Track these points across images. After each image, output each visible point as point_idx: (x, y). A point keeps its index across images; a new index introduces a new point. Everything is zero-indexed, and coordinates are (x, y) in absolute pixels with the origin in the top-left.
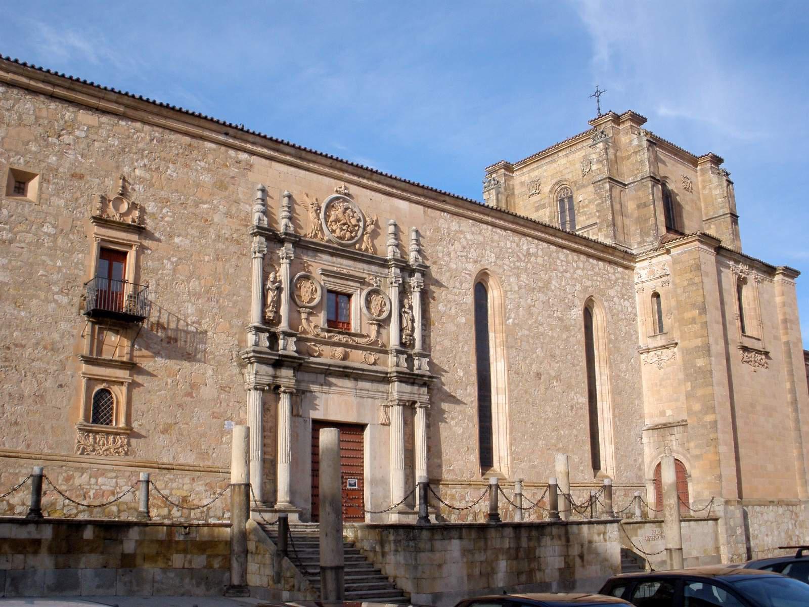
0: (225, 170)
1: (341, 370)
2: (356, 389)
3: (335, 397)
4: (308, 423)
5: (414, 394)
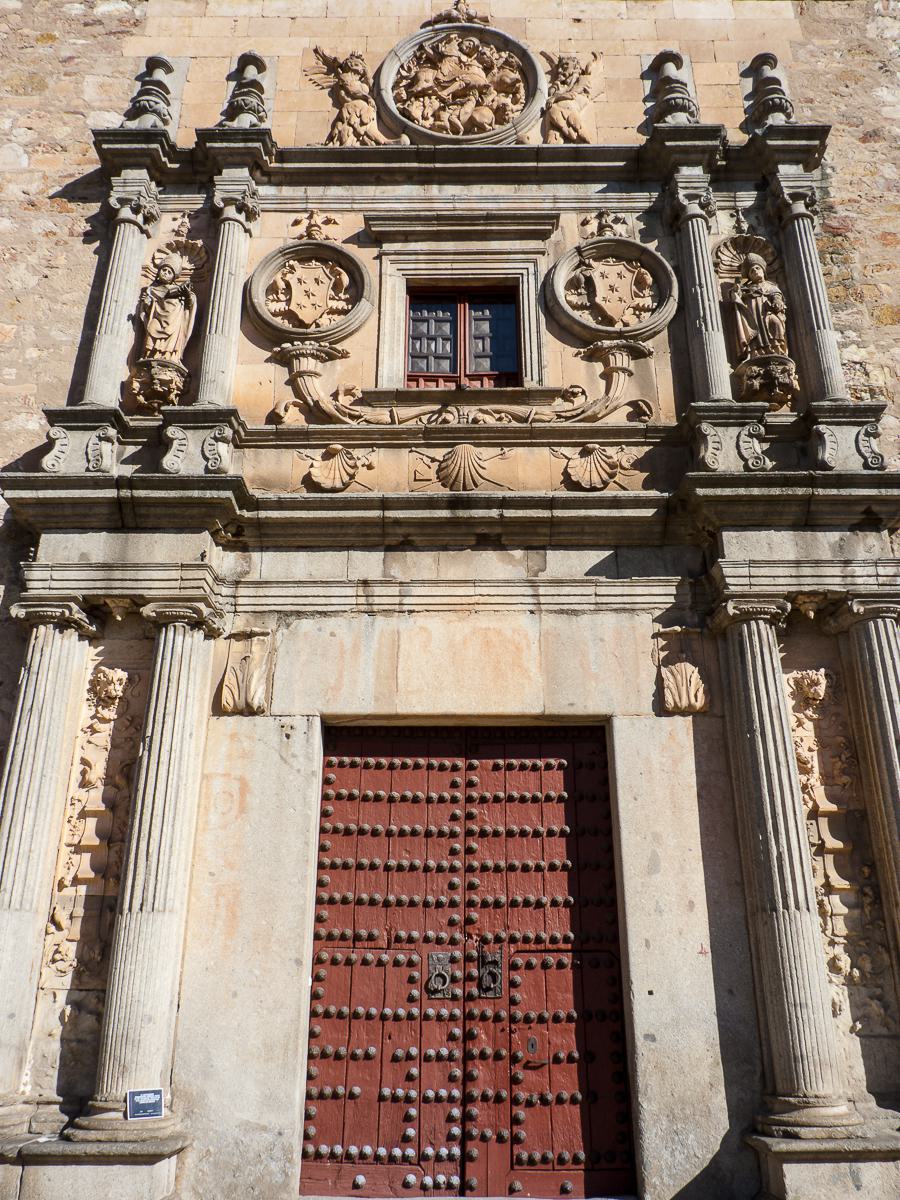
0: (43, 50)
1: (445, 513)
2: (533, 584)
3: (435, 623)
4: (298, 737)
5: (817, 563)
